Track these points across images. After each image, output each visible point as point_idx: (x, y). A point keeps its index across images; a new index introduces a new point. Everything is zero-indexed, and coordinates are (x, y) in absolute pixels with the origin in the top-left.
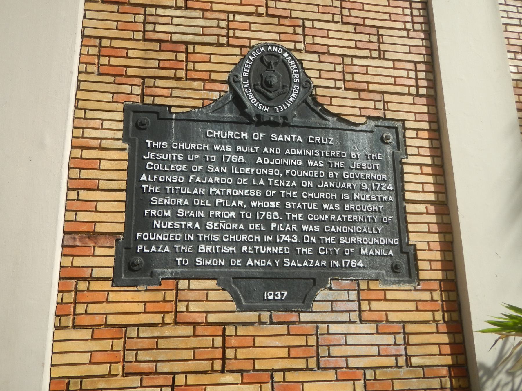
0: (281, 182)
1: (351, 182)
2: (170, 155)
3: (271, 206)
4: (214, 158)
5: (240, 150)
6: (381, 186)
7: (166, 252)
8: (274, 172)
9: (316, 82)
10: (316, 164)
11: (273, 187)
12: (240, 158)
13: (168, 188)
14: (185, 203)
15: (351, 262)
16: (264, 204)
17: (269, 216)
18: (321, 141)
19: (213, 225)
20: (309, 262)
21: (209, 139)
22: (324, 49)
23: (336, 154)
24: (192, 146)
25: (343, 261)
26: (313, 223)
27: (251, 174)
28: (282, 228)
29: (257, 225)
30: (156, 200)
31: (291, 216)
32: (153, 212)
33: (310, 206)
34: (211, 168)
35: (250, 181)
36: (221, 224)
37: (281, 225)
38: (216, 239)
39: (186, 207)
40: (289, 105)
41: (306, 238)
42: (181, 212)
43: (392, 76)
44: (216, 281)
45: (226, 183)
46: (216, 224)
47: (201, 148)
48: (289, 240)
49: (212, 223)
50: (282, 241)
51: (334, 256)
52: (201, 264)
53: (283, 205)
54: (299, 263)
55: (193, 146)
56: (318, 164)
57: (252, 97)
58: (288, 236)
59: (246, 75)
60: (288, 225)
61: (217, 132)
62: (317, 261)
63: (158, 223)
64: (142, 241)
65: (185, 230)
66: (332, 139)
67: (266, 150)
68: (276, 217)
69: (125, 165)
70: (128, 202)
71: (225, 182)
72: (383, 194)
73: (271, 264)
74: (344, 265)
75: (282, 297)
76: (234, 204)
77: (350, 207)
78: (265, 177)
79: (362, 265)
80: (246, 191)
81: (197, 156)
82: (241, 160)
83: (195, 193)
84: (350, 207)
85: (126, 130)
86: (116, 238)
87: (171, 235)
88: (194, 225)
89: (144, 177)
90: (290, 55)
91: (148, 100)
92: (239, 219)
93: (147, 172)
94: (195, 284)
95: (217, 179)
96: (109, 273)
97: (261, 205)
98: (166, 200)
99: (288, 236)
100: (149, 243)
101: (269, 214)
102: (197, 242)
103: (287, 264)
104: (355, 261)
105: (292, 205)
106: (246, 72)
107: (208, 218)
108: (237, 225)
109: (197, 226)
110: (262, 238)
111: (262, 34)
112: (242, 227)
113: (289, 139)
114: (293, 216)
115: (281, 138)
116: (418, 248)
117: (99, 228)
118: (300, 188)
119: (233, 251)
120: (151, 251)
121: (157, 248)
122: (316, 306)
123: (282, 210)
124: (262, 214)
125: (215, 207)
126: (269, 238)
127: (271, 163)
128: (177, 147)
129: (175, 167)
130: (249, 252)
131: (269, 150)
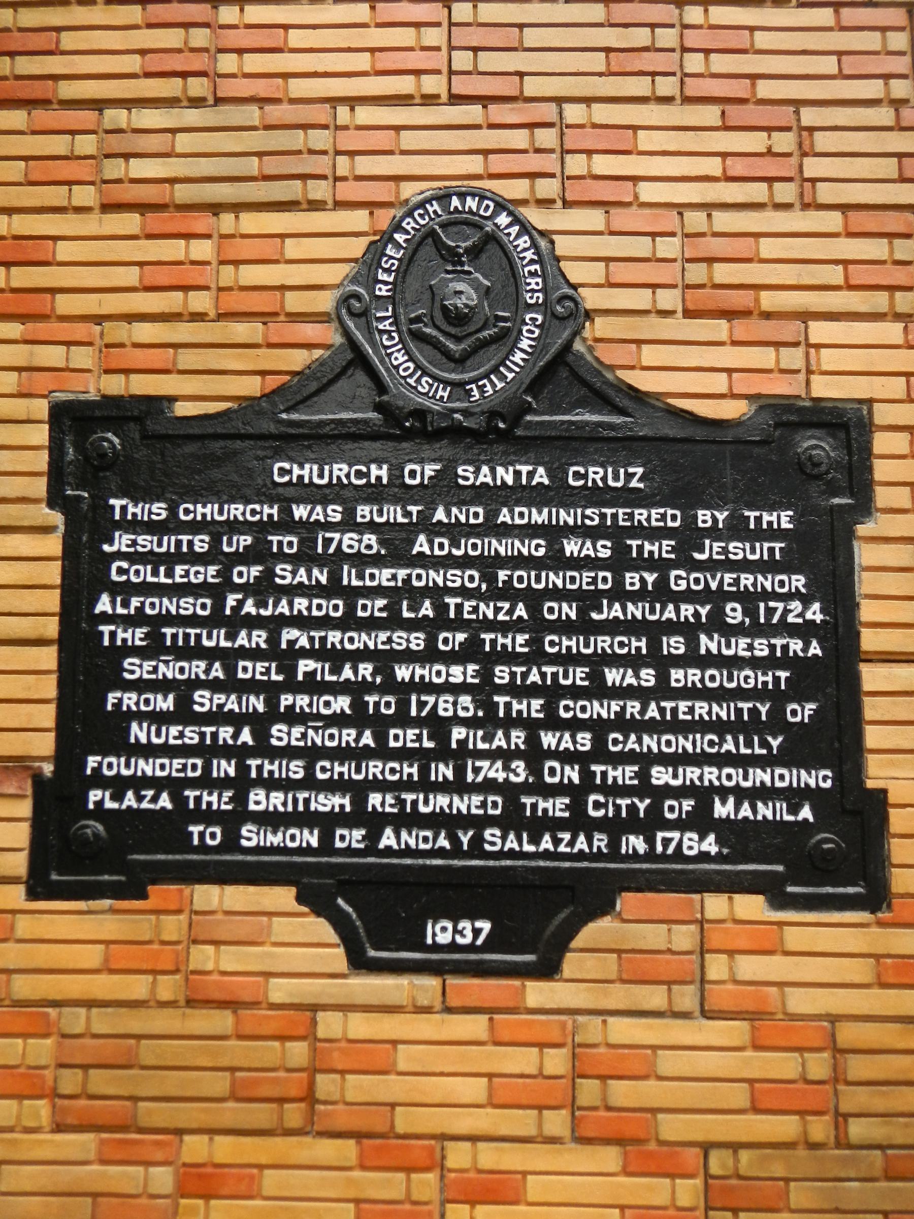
3: (451, 679)
4: (290, 542)
5: (368, 519)
6: (786, 611)
7: (163, 808)
8: (462, 578)
10: (588, 550)
11: (459, 624)
14: (213, 674)
17: (445, 708)
18: (604, 479)
19: (289, 734)
20: (557, 842)
21: (280, 490)
22: (623, 192)
23: (648, 519)
24: (233, 512)
25: (660, 835)
26: (575, 725)
27: (396, 587)
28: (484, 739)
30: (136, 668)
31: (508, 706)
32: (130, 700)
33: (566, 676)
35: (393, 609)
36: (311, 732)
37: (480, 733)
38: (295, 773)
39: (215, 686)
40: (510, 376)
41: (552, 772)
42: (203, 700)
43: (836, 262)
44: (293, 890)
45: (327, 614)
47: (258, 517)
48: (501, 776)
50: (480, 779)
52: (253, 844)
53: (486, 675)
54: (529, 842)
55: (236, 510)
56: (595, 550)
57: (401, 360)
58: (499, 764)
59: (384, 293)
60: (500, 733)
61: (302, 467)
62: (582, 838)
65: (209, 751)
66: (640, 471)
67: (440, 515)
68: (466, 709)
69: (53, 573)
71: (323, 612)
72: (791, 636)
74: (659, 848)
76: (347, 673)
77: (686, 677)
78: (437, 593)
79: (714, 850)
81: (246, 540)
82: (369, 547)
84: (686, 677)
85: (57, 474)
86: (31, 772)
88: (235, 736)
89: (104, 605)
91: (115, 385)
92: (358, 718)
93: (115, 590)
94: (237, 896)
95: (301, 604)
97: (422, 677)
98: (162, 668)
100: (119, 785)
101: (446, 702)
102: (241, 785)
103: (493, 844)
104: (695, 836)
105: (513, 675)
106: (386, 283)
107: (273, 715)
108: (353, 732)
109: (246, 736)
110: (424, 771)
111: (437, 155)
112: (367, 739)
113: (510, 480)
114: (516, 706)
116: (892, 798)
118: (537, 626)
119: (342, 807)
121: (140, 799)
122: (571, 964)
124: (426, 703)
126: (444, 771)
127: (455, 552)
128: (192, 515)
129: (187, 573)
131: (448, 514)
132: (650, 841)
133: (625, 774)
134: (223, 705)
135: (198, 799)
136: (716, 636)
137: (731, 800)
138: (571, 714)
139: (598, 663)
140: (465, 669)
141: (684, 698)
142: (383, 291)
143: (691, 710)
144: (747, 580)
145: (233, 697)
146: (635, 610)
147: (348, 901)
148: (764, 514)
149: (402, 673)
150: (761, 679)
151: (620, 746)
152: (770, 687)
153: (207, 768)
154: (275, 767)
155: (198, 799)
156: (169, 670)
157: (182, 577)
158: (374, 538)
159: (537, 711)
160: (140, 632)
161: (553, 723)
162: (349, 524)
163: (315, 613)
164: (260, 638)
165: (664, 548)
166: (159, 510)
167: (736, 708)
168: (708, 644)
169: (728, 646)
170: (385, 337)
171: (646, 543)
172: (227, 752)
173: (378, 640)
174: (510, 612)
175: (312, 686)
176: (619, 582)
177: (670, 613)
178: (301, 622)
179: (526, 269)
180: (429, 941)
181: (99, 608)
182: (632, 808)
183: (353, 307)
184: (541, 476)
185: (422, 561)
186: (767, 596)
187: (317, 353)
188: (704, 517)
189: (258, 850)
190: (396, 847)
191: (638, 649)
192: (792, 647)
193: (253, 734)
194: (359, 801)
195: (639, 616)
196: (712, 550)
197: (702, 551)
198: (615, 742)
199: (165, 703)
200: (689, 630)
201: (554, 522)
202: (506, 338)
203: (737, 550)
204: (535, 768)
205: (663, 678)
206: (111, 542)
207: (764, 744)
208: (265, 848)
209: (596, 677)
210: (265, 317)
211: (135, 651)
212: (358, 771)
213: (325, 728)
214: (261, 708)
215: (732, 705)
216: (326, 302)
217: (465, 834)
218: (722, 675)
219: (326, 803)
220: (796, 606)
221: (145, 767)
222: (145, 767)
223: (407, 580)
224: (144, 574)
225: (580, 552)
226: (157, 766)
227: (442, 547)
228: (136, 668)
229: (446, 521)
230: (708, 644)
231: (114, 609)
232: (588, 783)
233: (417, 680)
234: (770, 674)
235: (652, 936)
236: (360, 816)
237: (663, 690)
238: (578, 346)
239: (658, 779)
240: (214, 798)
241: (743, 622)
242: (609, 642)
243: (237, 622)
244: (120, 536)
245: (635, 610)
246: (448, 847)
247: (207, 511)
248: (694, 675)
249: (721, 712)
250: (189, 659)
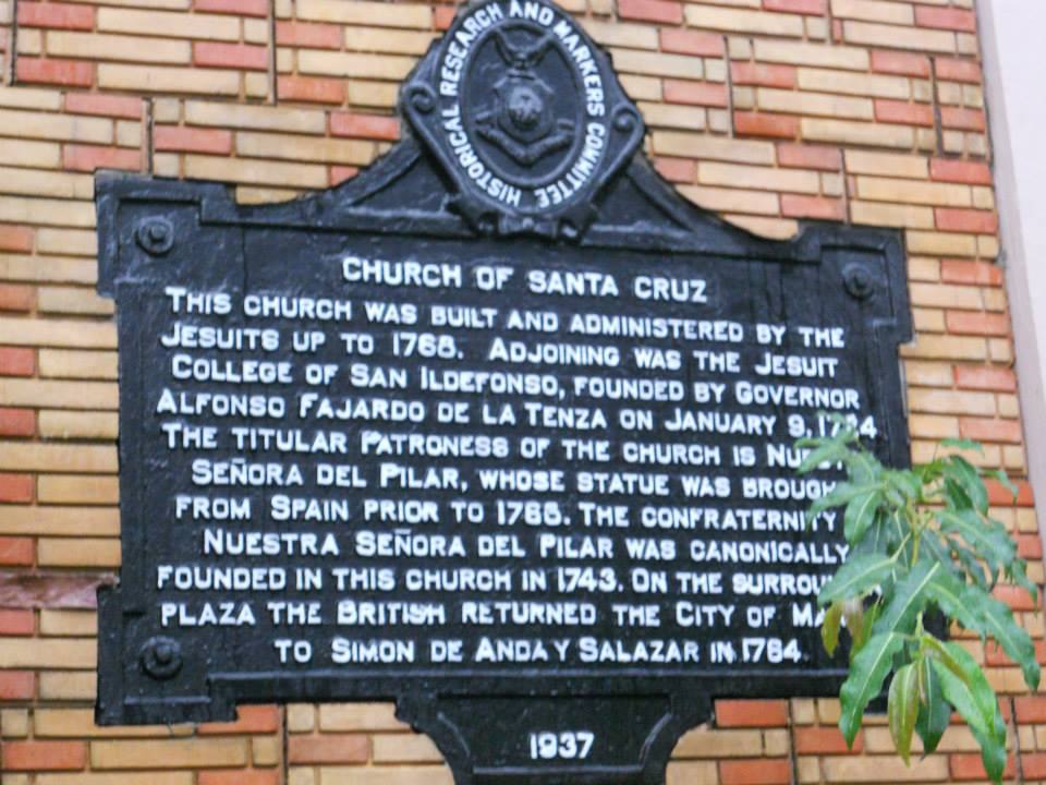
2: (239, 333)
4: (365, 342)
9: (651, 115)
11: (540, 431)
16: (519, 480)
17: (532, 513)
20: (650, 650)
26: (658, 533)
30: (205, 471)
32: (201, 505)
34: (360, 375)
35: (474, 413)
39: (293, 491)
42: (281, 507)
43: (867, 97)
48: (591, 585)
50: (571, 587)
51: (720, 631)
53: (570, 481)
55: (306, 306)
58: (589, 572)
64: (171, 592)
65: (291, 560)
68: (552, 516)
69: (110, 365)
70: (126, 472)
74: (746, 656)
76: (432, 479)
77: (758, 486)
78: (517, 399)
81: (318, 338)
82: (446, 350)
84: (758, 486)
86: (99, 583)
88: (319, 544)
89: (166, 402)
90: (575, 30)
91: (166, 166)
92: (446, 525)
93: (178, 385)
94: (336, 715)
95: (380, 406)
96: (87, 686)
98: (234, 471)
100: (194, 600)
102: (328, 596)
105: (596, 483)
107: (357, 522)
109: (331, 545)
110: (517, 580)
112: (457, 547)
115: (556, 284)
117: (50, 553)
118: (616, 435)
119: (436, 618)
120: (202, 622)
121: (219, 612)
123: (568, 498)
124: (512, 510)
125: (375, 491)
126: (535, 580)
132: (738, 648)
133: (709, 582)
134: (305, 512)
135: (284, 613)
139: (677, 470)
141: (757, 507)
142: (448, 89)
144: (806, 394)
145: (314, 503)
146: (707, 421)
147: (448, 716)
149: (488, 479)
153: (291, 577)
155: (284, 613)
156: (243, 474)
160: (209, 432)
161: (637, 530)
162: (423, 325)
164: (338, 441)
165: (729, 362)
166: (222, 303)
168: (776, 455)
172: (312, 560)
173: (462, 446)
174: (589, 419)
175: (396, 491)
176: (689, 392)
177: (738, 424)
178: (383, 425)
180: (534, 755)
182: (719, 616)
183: (417, 105)
184: (610, 286)
185: (500, 365)
187: (385, 148)
188: (764, 333)
189: (351, 664)
190: (493, 659)
193: (339, 541)
194: (454, 611)
196: (771, 364)
198: (698, 550)
199: (242, 510)
200: (757, 441)
202: (568, 148)
203: (796, 365)
204: (623, 577)
205: (736, 487)
206: (171, 333)
209: (675, 485)
210: (329, 105)
211: (205, 453)
212: (450, 579)
213: (412, 535)
214: (345, 515)
216: (390, 96)
217: (561, 643)
218: (790, 486)
219: (419, 614)
221: (223, 578)
222: (223, 578)
223: (487, 385)
224: (208, 369)
227: (518, 353)
228: (205, 471)
230: (776, 455)
232: (674, 593)
235: (748, 742)
236: (454, 628)
237: (736, 500)
238: (638, 160)
240: (300, 610)
243: (313, 425)
244: (181, 330)
245: (707, 421)
247: (271, 304)
249: (793, 521)
250: (265, 463)
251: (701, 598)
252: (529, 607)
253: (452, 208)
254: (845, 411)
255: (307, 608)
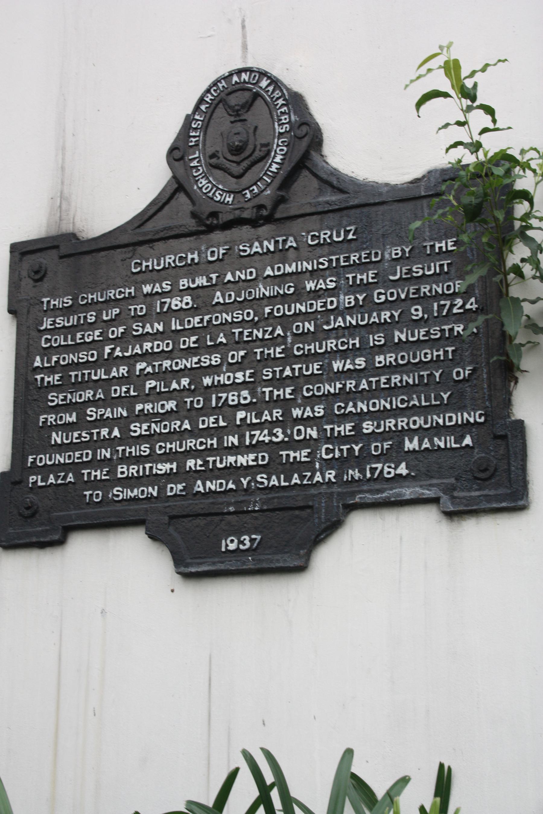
0: (255, 331)
1: (389, 309)
3: (237, 381)
6: (452, 306)
8: (243, 315)
12: (185, 301)
13: (73, 374)
14: (98, 396)
15: (383, 468)
17: (232, 398)
19: (140, 428)
20: (302, 477)
26: (312, 401)
27: (203, 327)
29: (212, 419)
32: (51, 418)
34: (138, 329)
36: (153, 425)
46: (145, 426)
48: (267, 439)
49: (138, 425)
50: (254, 442)
55: (111, 294)
56: (326, 284)
58: (266, 432)
63: (58, 436)
64: (34, 469)
66: (353, 228)
67: (229, 277)
68: (245, 398)
73: (233, 487)
74: (368, 475)
75: (252, 545)
77: (385, 359)
80: (195, 359)
83: (114, 377)
84: (385, 359)
87: (77, 454)
88: (110, 433)
95: (147, 346)
99: (266, 432)
101: (233, 395)
105: (274, 372)
109: (116, 433)
112: (187, 426)
119: (171, 469)
124: (221, 398)
127: (238, 299)
130: (198, 468)
131: (234, 275)
133: (346, 429)
136: (405, 330)
137: (416, 439)
138: (311, 393)
140: (245, 373)
143: (389, 380)
145: (109, 410)
148: (436, 243)
150: (435, 354)
151: (343, 411)
152: (442, 358)
154: (133, 450)
157: (80, 339)
158: (189, 298)
159: (290, 394)
163: (156, 350)
164: (123, 370)
166: (68, 301)
167: (419, 375)
168: (399, 335)
169: (413, 335)
170: (194, 170)
171: (358, 275)
173: (191, 362)
174: (272, 333)
175: (155, 396)
179: (279, 111)
181: (36, 364)
186: (437, 297)
191: (354, 345)
192: (456, 329)
195: (354, 323)
197: (395, 274)
201: (299, 270)
207: (438, 397)
208: (126, 500)
209: (326, 368)
213: (160, 422)
214: (125, 414)
215: (416, 374)
218: (409, 355)
219: (164, 468)
220: (459, 302)
221: (60, 459)
223: (210, 321)
225: (316, 287)
226: (67, 457)
228: (56, 399)
229: (232, 280)
231: (43, 364)
233: (216, 383)
234: (442, 350)
239: (367, 429)
241: (423, 317)
242: (335, 343)
246: (234, 488)
248: (391, 358)
251: (342, 439)
252: (226, 459)
253: (194, 215)
254: (455, 295)
255: (102, 471)
